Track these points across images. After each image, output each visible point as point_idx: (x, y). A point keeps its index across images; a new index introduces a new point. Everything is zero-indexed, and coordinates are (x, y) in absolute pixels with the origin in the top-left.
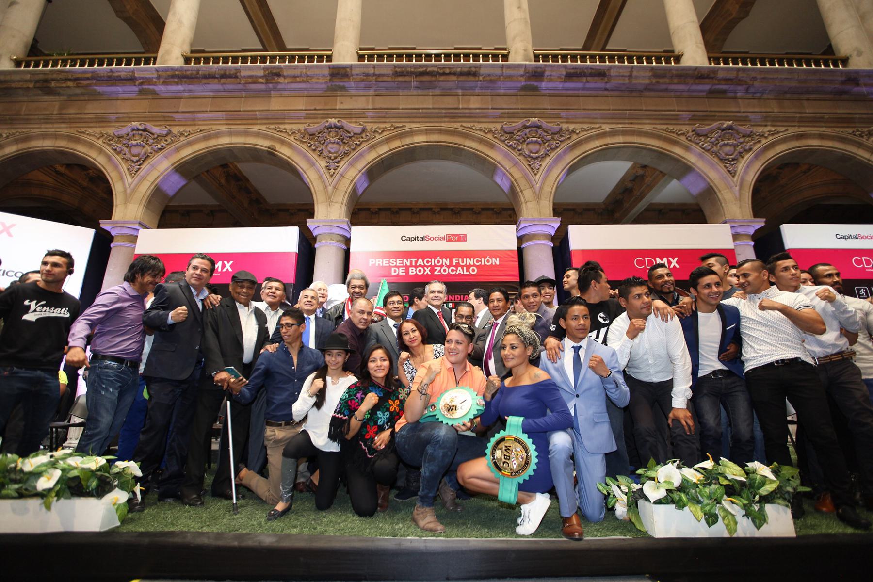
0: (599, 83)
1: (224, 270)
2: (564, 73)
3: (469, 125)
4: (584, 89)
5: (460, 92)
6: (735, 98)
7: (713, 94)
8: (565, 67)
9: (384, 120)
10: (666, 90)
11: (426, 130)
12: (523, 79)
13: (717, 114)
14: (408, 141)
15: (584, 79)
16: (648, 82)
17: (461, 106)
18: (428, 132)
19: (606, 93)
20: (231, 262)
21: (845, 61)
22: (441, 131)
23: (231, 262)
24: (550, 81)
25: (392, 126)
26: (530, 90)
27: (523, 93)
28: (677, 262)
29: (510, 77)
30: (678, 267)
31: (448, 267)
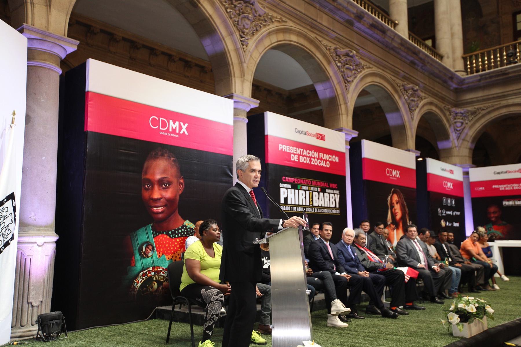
0: (378, 35)
1: (182, 132)
2: (371, 23)
3: (320, 39)
4: (371, 36)
5: (318, 6)
6: (417, 69)
7: (413, 64)
8: (373, 18)
9: (275, 9)
10: (398, 53)
11: (299, 32)
12: (352, 15)
13: (412, 78)
14: (313, 49)
15: (376, 31)
16: (396, 45)
17: (318, 21)
18: (299, 34)
19: (377, 43)
20: (186, 125)
21: (441, 57)
22: (305, 37)
23: (186, 125)
24: (363, 25)
25: (281, 18)
26: (350, 23)
27: (345, 24)
28: (187, 129)
29: (348, 11)
30: (186, 133)
31: (318, 159)
